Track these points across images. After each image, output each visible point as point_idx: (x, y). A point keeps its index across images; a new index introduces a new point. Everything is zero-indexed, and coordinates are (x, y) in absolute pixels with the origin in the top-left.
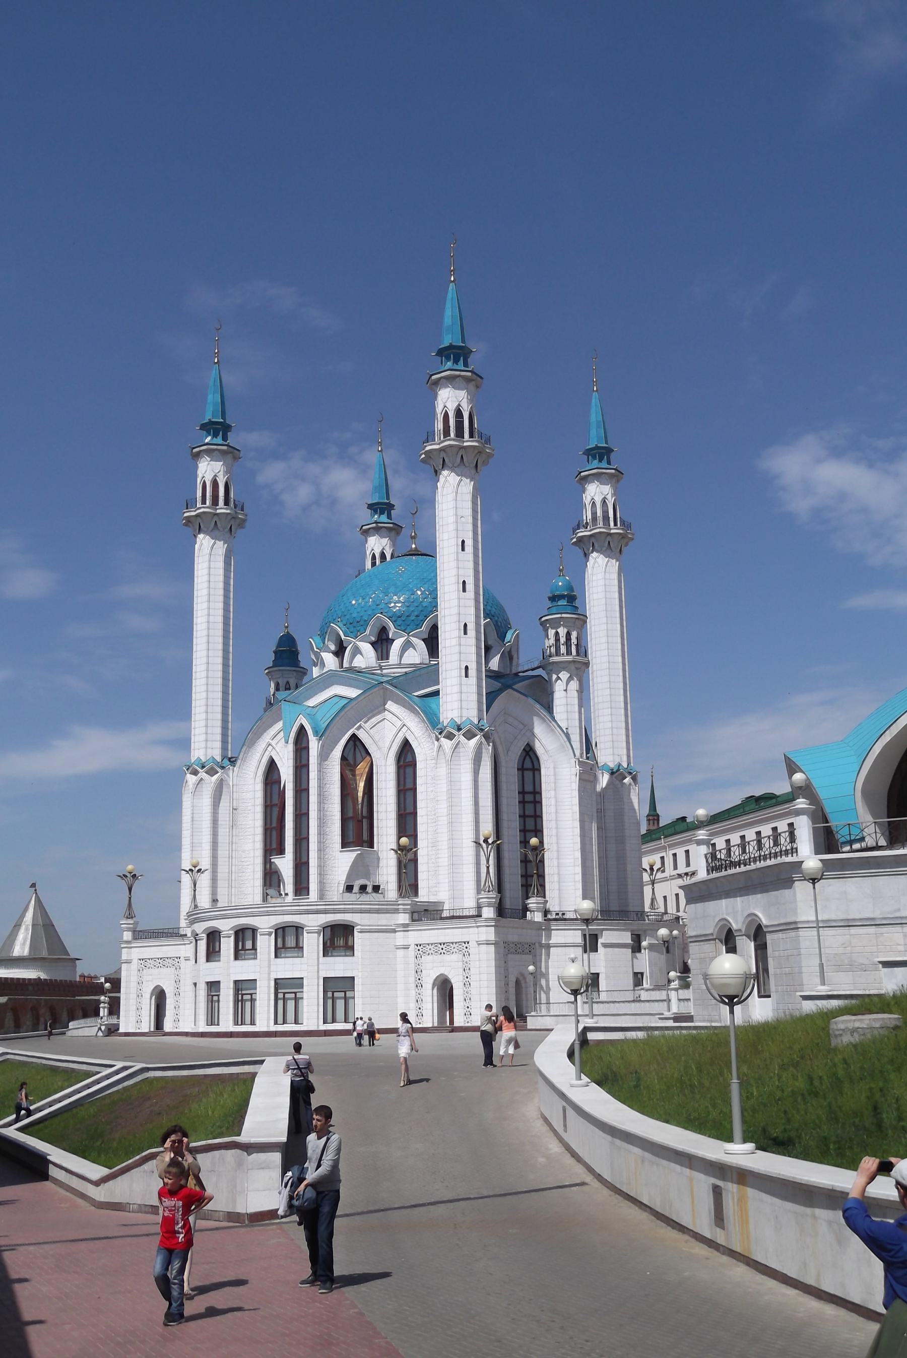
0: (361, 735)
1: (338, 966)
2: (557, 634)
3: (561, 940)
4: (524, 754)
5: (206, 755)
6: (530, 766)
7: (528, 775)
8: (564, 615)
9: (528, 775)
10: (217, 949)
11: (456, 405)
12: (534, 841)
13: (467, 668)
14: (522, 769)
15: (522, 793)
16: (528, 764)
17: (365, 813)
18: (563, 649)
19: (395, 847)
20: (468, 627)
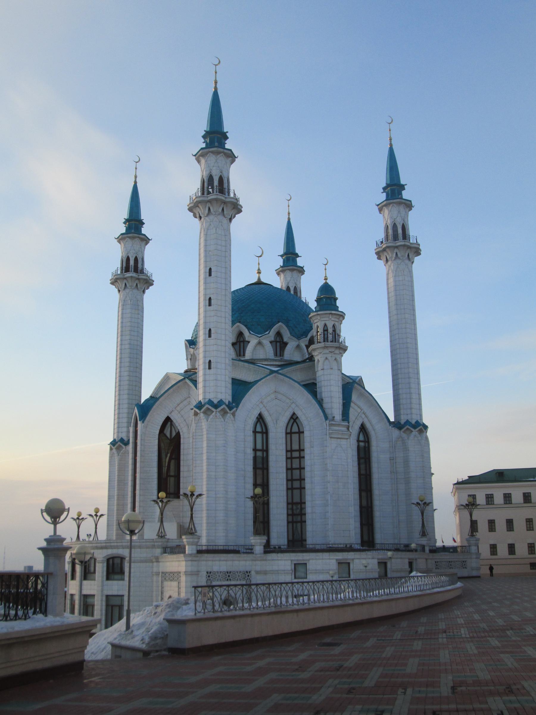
0: (175, 417)
1: (116, 587)
3: (275, 568)
4: (292, 421)
5: (118, 437)
6: (297, 431)
7: (295, 437)
8: (319, 313)
10: (92, 569)
11: (208, 172)
12: (259, 491)
13: (210, 361)
14: (289, 433)
15: (289, 451)
16: (295, 429)
17: (172, 473)
19: (155, 498)
20: (212, 332)
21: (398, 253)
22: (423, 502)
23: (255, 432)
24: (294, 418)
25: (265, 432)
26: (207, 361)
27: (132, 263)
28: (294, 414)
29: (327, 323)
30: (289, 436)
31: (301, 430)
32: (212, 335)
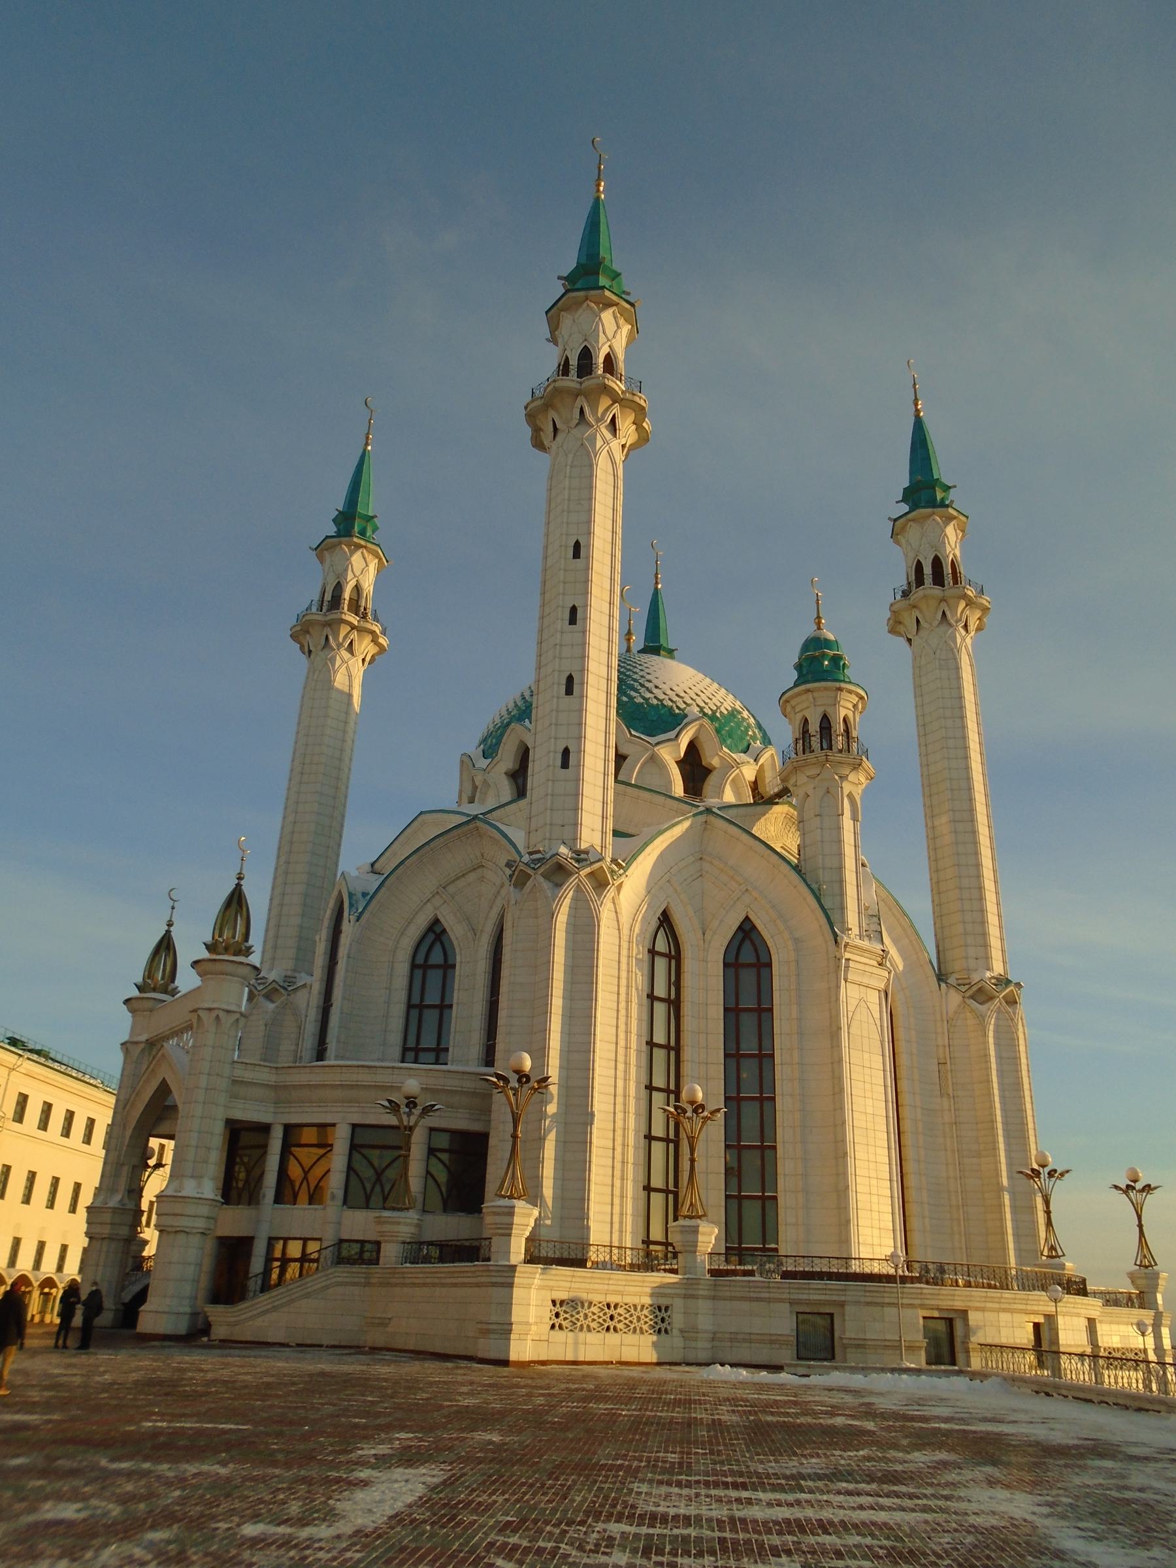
2: (806, 721)
4: (741, 935)
6: (753, 960)
7: (748, 978)
9: (748, 978)
14: (732, 964)
16: (747, 956)
18: (815, 742)
21: (948, 614)
22: (1047, 1170)
23: (652, 952)
24: (747, 931)
25: (675, 956)
26: (561, 748)
27: (347, 595)
28: (747, 918)
29: (830, 711)
30: (732, 971)
31: (764, 960)
32: (576, 688)
